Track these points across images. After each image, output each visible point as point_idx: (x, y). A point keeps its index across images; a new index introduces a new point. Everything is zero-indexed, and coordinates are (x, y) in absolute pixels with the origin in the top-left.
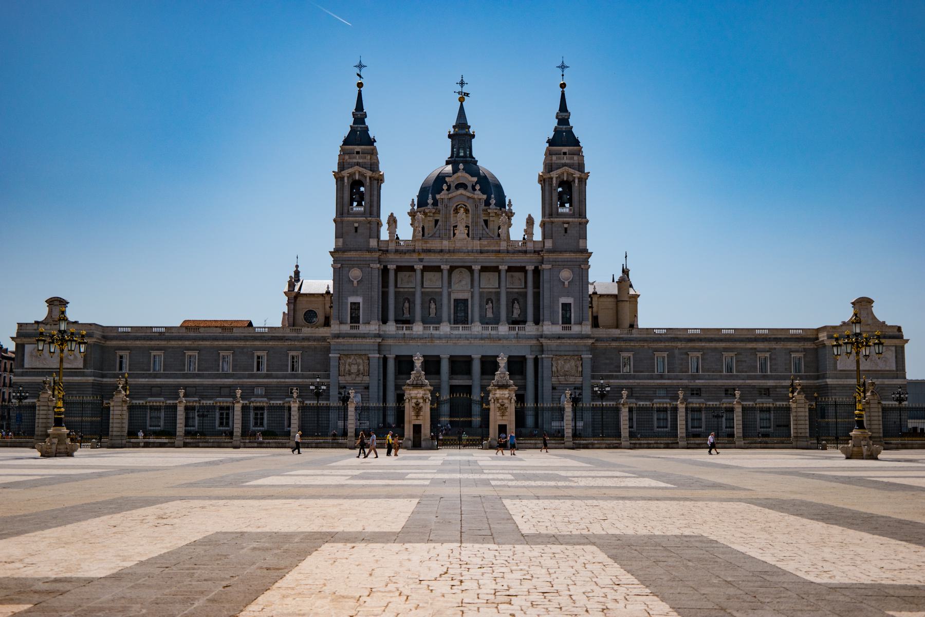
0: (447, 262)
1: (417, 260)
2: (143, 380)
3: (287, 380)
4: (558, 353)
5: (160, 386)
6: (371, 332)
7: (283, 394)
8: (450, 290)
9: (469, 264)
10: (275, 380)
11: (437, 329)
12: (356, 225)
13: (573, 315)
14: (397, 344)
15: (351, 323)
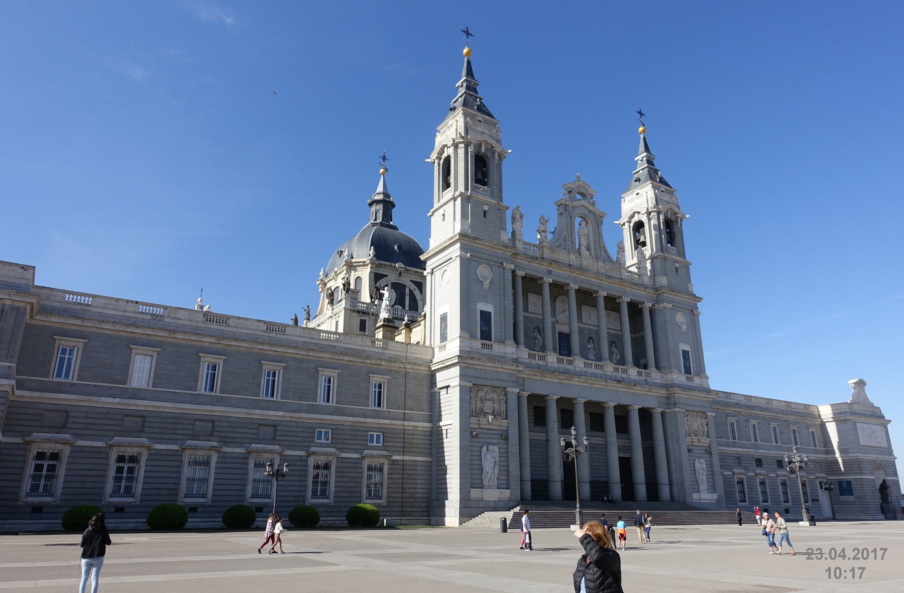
0: (575, 281)
1: (546, 271)
2: (110, 400)
3: (368, 420)
4: (688, 408)
5: (143, 416)
6: (507, 355)
7: (359, 442)
8: (554, 320)
9: (595, 288)
10: (351, 419)
11: (570, 363)
12: (486, 208)
13: (691, 364)
14: (531, 377)
15: (481, 339)
